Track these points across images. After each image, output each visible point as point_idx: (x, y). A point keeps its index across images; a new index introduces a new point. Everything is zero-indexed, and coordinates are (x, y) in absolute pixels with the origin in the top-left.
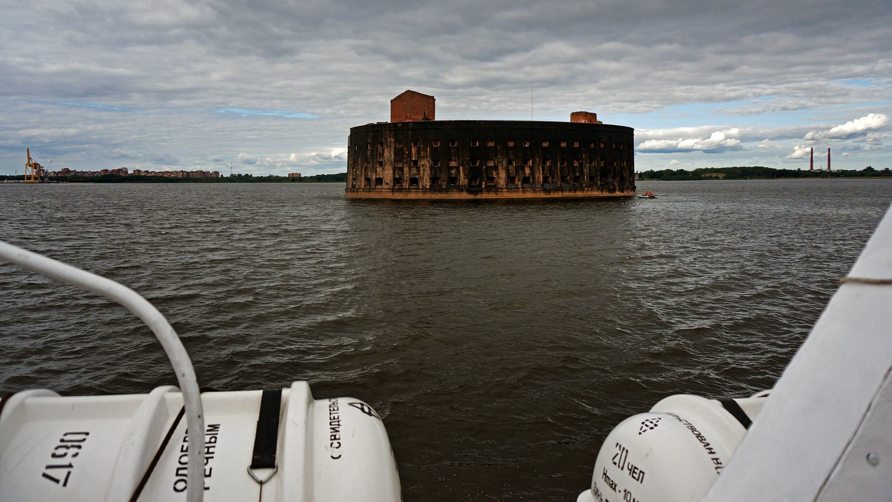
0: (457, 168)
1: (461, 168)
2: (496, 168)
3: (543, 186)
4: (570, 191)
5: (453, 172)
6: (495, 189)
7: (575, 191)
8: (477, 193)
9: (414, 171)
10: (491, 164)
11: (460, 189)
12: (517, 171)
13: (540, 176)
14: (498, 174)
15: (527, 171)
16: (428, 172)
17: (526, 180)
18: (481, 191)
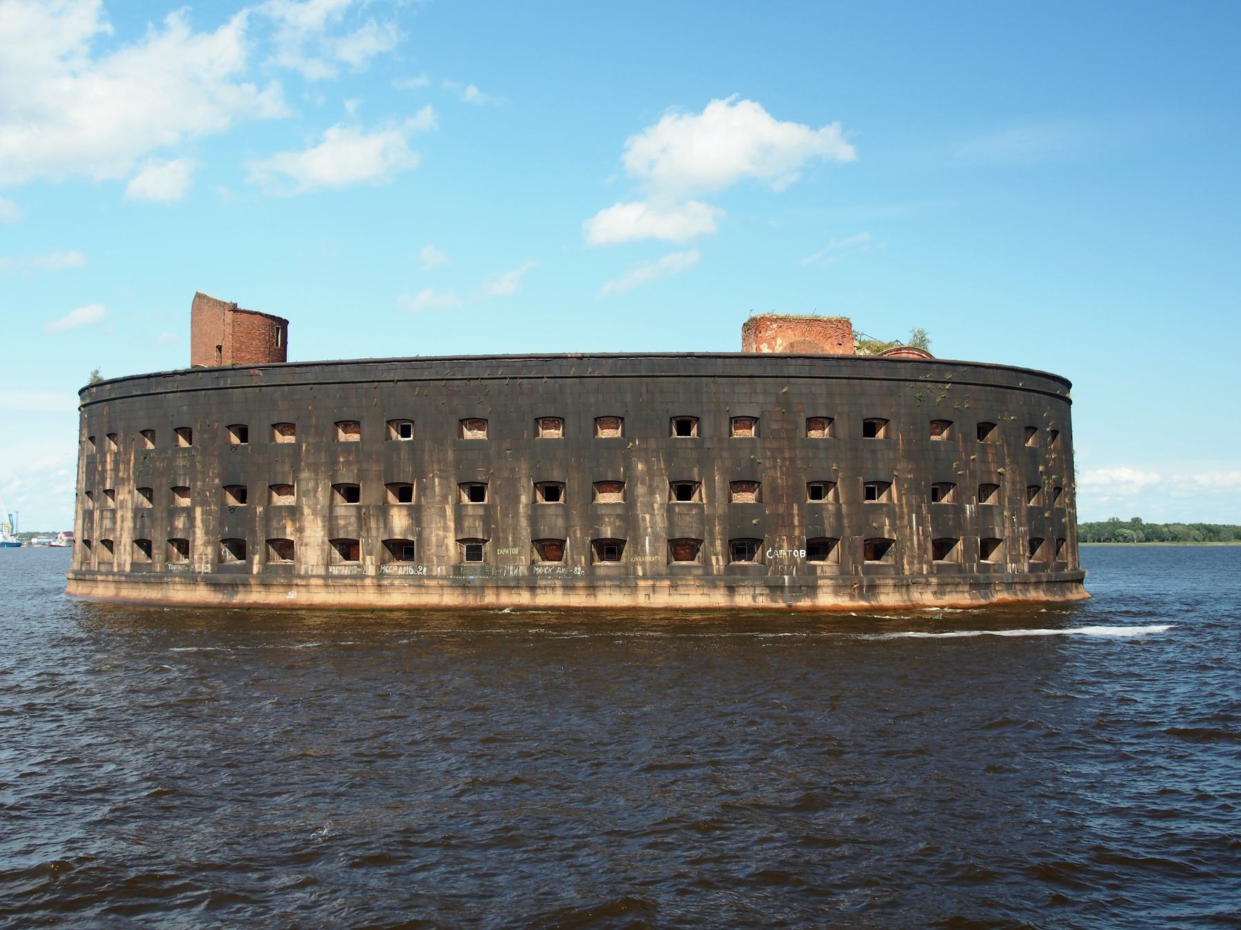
0: (189, 512)
1: (198, 511)
2: (294, 512)
3: (457, 569)
4: (568, 588)
5: (180, 523)
6: (290, 578)
7: (592, 588)
8: (233, 586)
9: (107, 523)
10: (281, 500)
11: (191, 578)
12: (362, 521)
13: (443, 540)
14: (300, 530)
16: (129, 524)
17: (402, 550)
18: (246, 585)
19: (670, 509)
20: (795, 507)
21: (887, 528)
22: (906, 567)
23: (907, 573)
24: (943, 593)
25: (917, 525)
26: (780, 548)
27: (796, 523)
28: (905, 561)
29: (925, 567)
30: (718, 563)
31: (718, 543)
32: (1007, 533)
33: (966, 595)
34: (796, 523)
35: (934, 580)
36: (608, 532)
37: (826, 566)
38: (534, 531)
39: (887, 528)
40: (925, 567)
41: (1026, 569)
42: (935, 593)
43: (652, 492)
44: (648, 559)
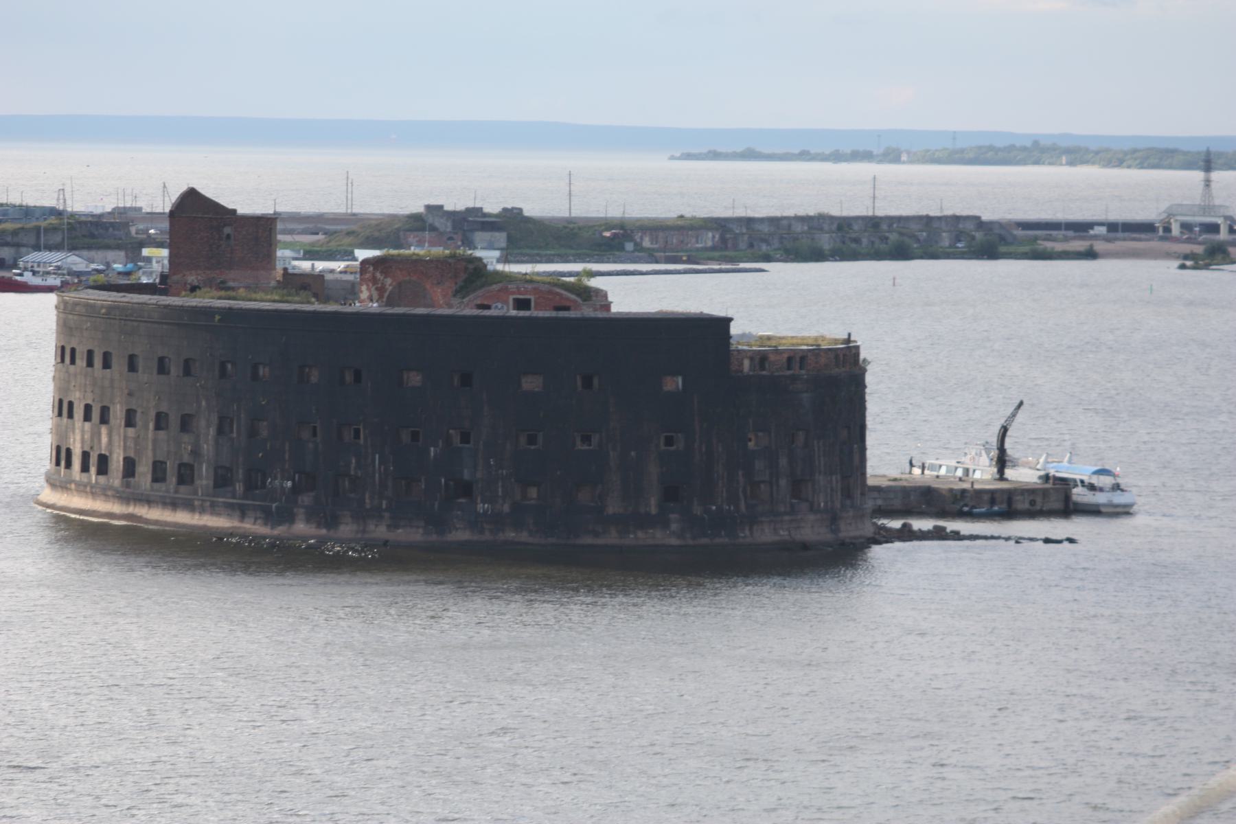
15: (104, 439)
19: (217, 442)
20: (287, 445)
21: (353, 465)
22: (367, 501)
23: (368, 506)
24: (397, 527)
25: (380, 464)
26: (276, 478)
27: (287, 457)
28: (367, 496)
29: (384, 503)
30: (239, 488)
31: (241, 471)
32: (479, 475)
33: (421, 530)
34: (287, 457)
35: (387, 515)
36: (186, 459)
37: (306, 499)
38: (155, 455)
39: (353, 465)
40: (384, 503)
41: (506, 508)
42: (389, 526)
43: (208, 427)
44: (204, 482)
